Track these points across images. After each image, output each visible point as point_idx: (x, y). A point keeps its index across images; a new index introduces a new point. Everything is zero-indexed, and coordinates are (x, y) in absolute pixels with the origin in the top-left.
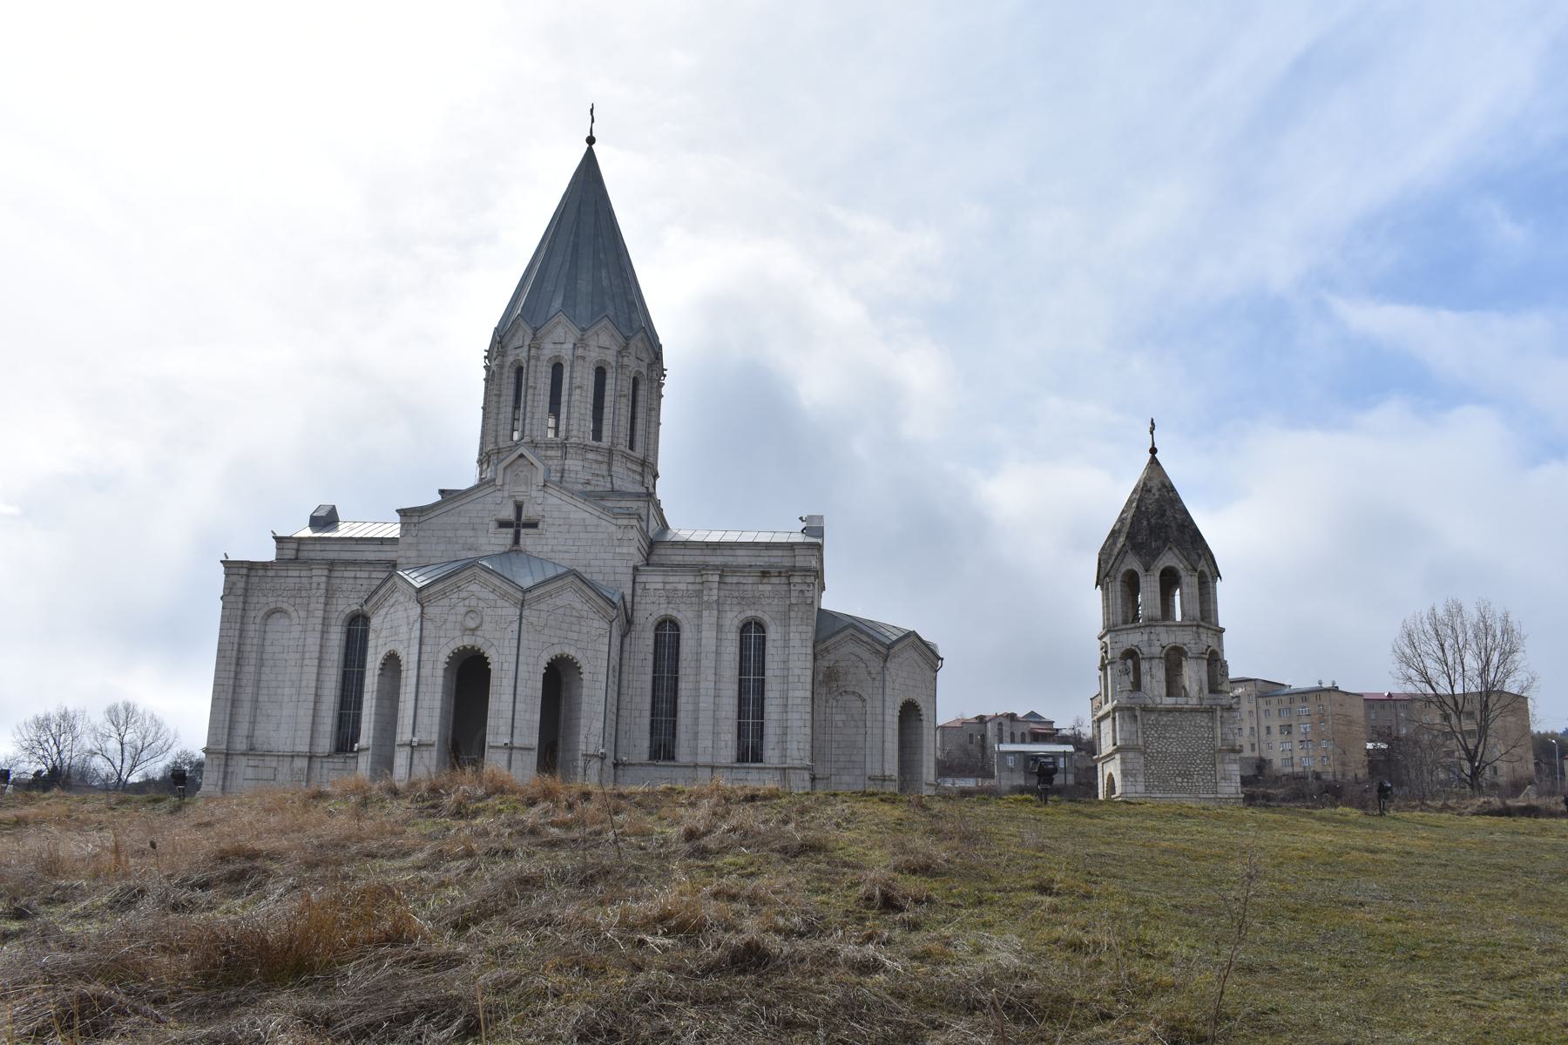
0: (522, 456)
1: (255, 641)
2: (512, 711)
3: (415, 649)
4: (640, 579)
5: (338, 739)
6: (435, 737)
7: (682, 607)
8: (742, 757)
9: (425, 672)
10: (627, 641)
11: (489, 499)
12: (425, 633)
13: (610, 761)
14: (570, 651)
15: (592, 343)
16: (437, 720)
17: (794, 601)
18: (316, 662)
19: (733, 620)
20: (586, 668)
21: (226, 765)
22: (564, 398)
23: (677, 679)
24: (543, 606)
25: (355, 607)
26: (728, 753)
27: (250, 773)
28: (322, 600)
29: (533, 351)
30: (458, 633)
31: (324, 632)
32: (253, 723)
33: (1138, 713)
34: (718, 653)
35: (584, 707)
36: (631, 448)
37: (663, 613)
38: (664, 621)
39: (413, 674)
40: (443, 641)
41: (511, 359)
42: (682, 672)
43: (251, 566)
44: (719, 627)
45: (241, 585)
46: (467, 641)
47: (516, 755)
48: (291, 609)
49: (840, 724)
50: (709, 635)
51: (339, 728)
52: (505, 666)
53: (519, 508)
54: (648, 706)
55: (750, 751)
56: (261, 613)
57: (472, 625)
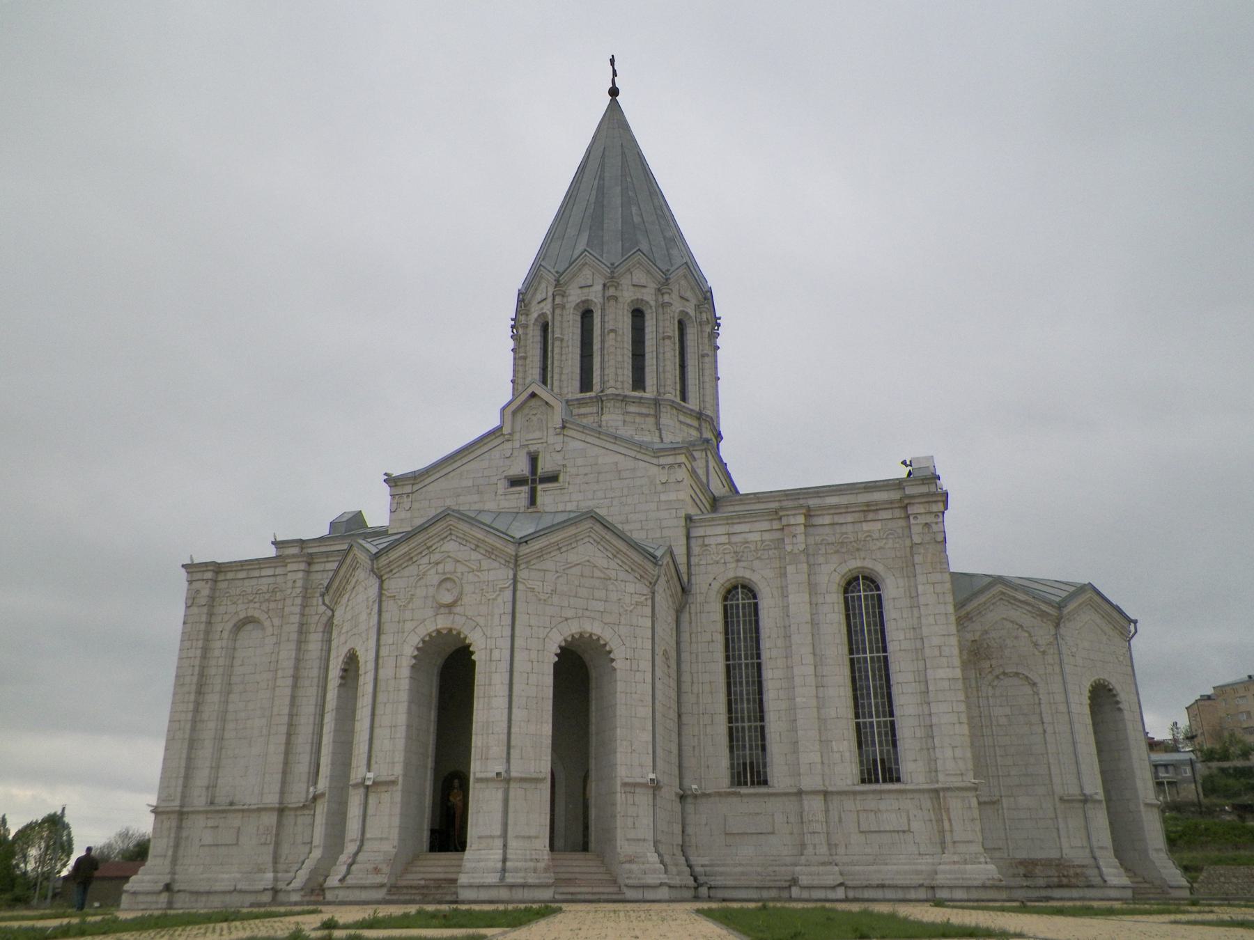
0: (533, 395)
1: (221, 661)
2: (512, 726)
3: (372, 643)
4: (696, 532)
6: (398, 770)
7: (757, 564)
8: (868, 776)
10: (685, 617)
11: (496, 454)
12: (385, 616)
13: (670, 792)
14: (594, 628)
15: (625, 282)
16: (401, 743)
17: (917, 539)
18: (289, 682)
19: (832, 575)
20: (619, 653)
21: (180, 828)
23: (759, 666)
24: (549, 565)
26: (846, 770)
27: (208, 838)
28: (298, 601)
29: (558, 300)
30: (430, 612)
32: (216, 768)
34: (814, 624)
35: (621, 710)
36: (684, 398)
37: (731, 575)
39: (371, 676)
40: (409, 626)
41: (535, 315)
42: (765, 655)
43: (218, 569)
45: (206, 592)
46: (443, 623)
47: (516, 791)
48: (263, 617)
49: (1003, 721)
50: (798, 601)
52: (496, 655)
53: (533, 460)
54: (722, 707)
56: (230, 625)
57: (447, 598)
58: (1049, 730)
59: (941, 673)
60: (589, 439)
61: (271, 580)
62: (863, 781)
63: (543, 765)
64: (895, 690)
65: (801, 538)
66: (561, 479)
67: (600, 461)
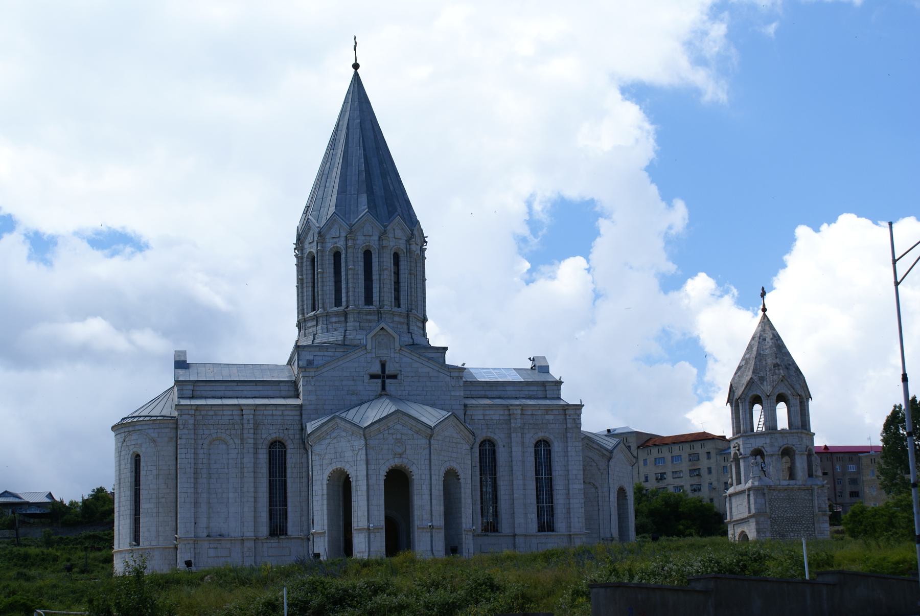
2: (426, 506)
3: (362, 467)
4: (469, 413)
5: (270, 527)
6: (383, 523)
8: (541, 529)
9: (372, 482)
12: (370, 457)
14: (455, 465)
19: (531, 439)
22: (375, 277)
25: (274, 436)
31: (255, 453)
33: (766, 491)
38: (485, 441)
44: (523, 444)
45: (192, 422)
46: (397, 462)
51: (270, 519)
52: (423, 477)
53: (383, 366)
55: (546, 524)
57: (399, 450)
58: (601, 508)
59: (576, 486)
60: (414, 358)
61: (231, 417)
62: (539, 531)
63: (442, 523)
64: (554, 492)
65: (519, 421)
66: (399, 377)
67: (420, 370)
